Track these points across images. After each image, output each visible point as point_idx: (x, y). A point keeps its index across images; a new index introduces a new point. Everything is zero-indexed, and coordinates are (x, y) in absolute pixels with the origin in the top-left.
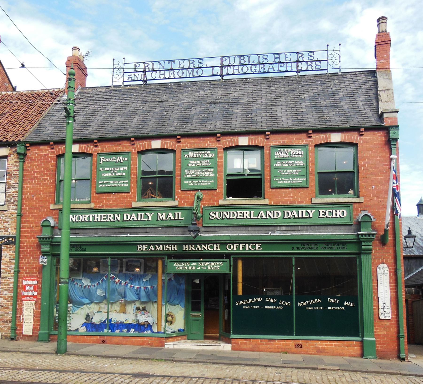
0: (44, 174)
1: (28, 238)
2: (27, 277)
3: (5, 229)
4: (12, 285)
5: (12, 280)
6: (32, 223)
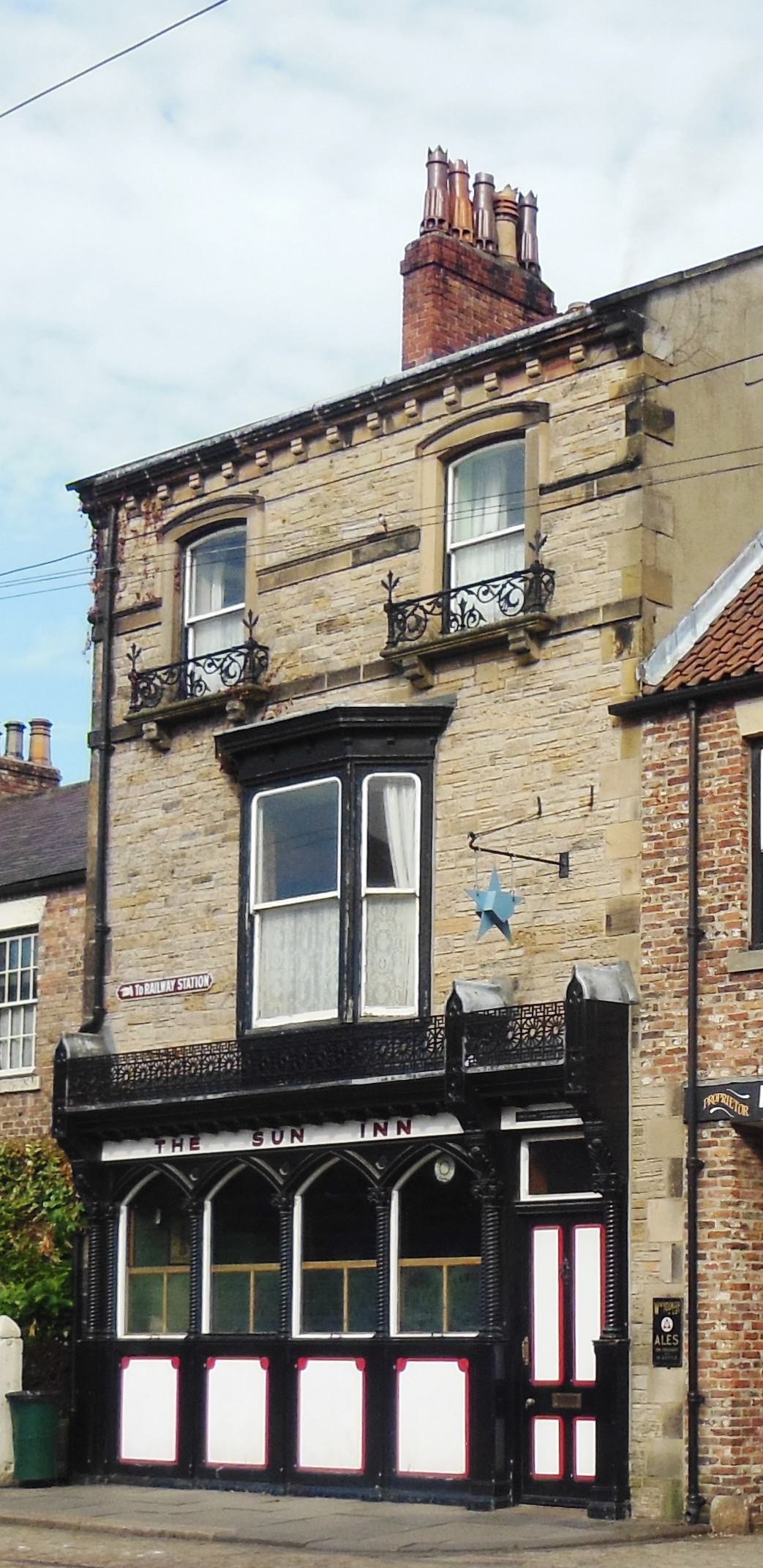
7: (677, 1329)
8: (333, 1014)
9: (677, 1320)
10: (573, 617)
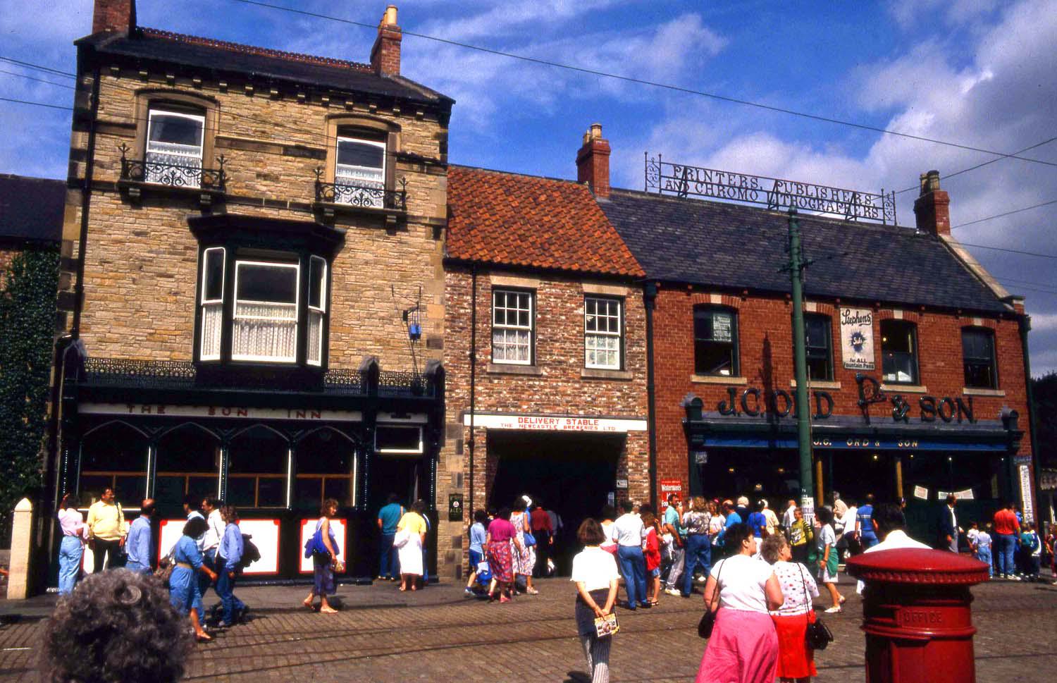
0: (679, 330)
1: (663, 423)
2: (666, 479)
3: (630, 407)
4: (646, 492)
5: (646, 485)
6: (667, 401)
7: (461, 506)
8: (292, 359)
9: (461, 502)
10: (413, 217)
